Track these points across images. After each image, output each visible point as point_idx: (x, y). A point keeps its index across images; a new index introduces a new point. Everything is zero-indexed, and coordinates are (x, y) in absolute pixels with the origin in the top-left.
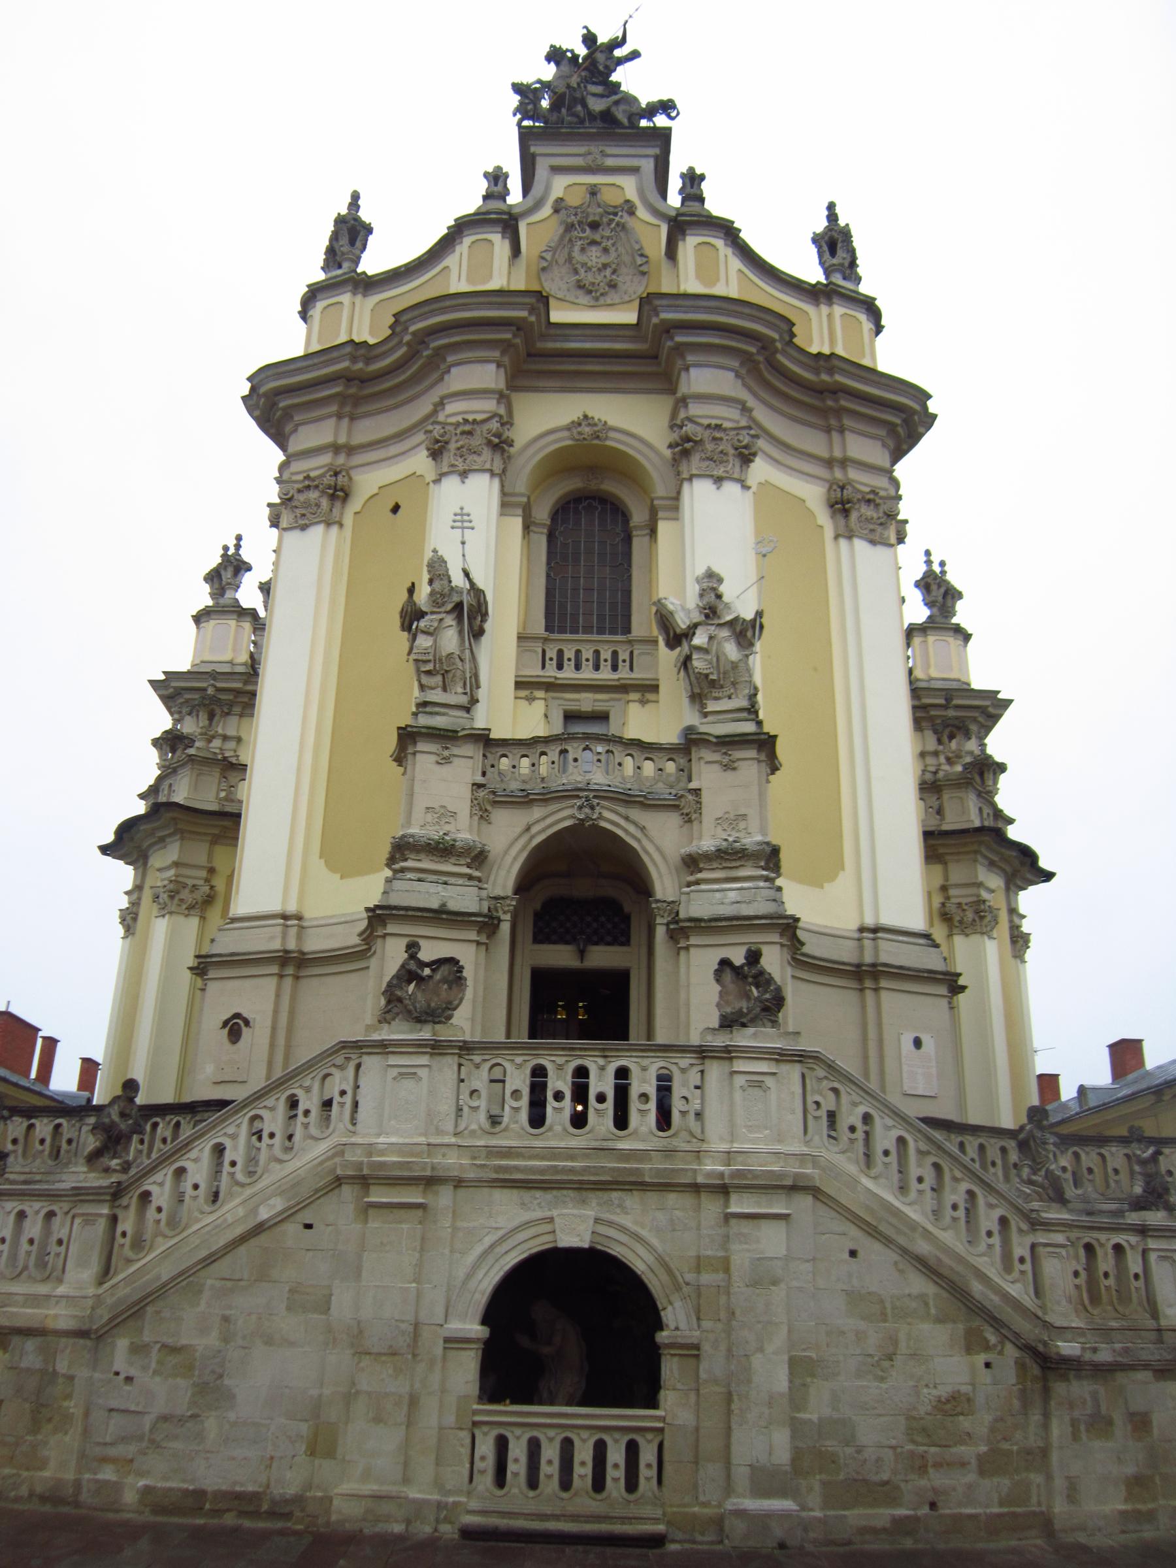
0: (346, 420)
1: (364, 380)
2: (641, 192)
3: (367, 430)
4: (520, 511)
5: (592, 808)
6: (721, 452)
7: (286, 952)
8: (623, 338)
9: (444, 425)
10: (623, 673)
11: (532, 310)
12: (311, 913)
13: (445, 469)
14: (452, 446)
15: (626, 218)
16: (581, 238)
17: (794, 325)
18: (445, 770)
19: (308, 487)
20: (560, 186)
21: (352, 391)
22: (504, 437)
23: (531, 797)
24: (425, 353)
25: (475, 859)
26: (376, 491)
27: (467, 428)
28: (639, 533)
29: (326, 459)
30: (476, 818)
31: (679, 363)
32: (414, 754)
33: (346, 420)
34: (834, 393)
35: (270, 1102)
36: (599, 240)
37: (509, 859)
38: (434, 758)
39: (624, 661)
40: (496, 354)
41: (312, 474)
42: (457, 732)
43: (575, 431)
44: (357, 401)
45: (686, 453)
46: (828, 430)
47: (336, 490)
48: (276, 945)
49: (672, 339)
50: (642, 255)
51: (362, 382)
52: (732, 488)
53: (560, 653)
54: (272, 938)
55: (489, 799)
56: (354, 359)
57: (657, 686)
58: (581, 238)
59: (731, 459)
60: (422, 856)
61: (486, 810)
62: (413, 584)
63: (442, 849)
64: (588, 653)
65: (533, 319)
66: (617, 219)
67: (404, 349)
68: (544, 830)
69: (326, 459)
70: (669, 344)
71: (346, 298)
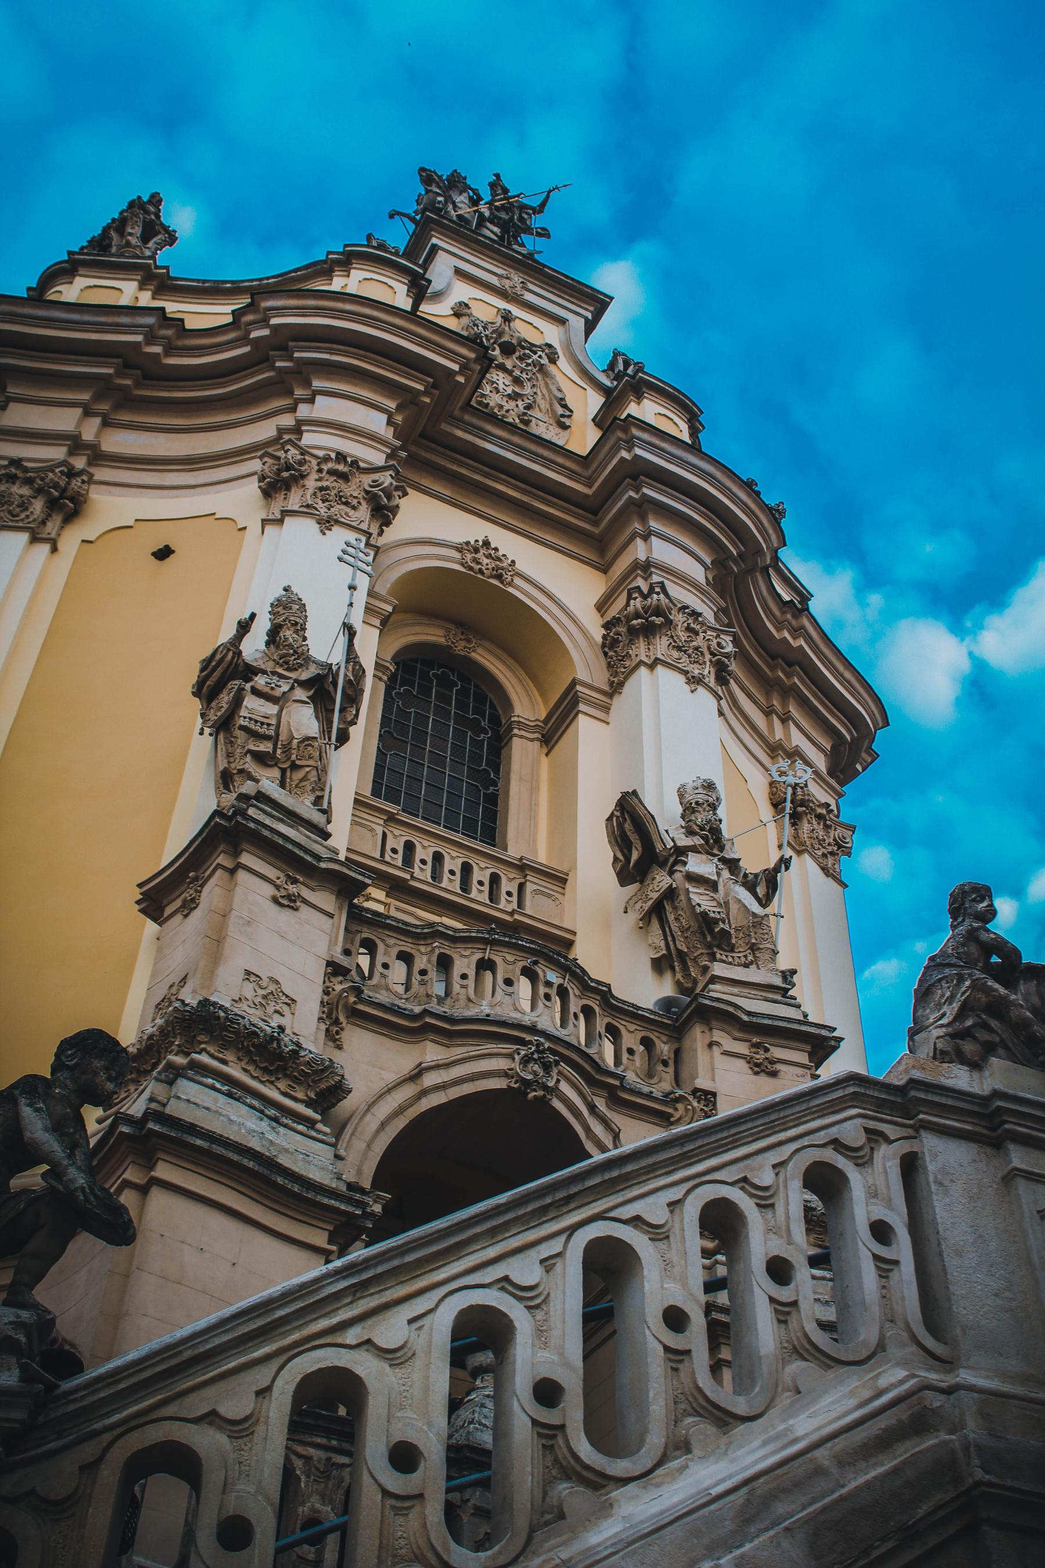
0: (97, 421)
1: (153, 373)
2: (568, 345)
4: (377, 622)
5: (547, 1067)
6: (697, 649)
8: (561, 469)
9: (303, 452)
11: (464, 368)
13: (296, 508)
14: (311, 483)
15: (545, 361)
17: (785, 545)
18: (284, 918)
20: (463, 292)
21: (128, 382)
22: (394, 503)
23: (428, 1020)
25: (321, 1094)
26: (131, 523)
27: (341, 467)
28: (523, 733)
29: (57, 453)
30: (323, 1027)
31: (637, 526)
32: (232, 872)
33: (97, 421)
34: (790, 665)
35: (653, 1209)
36: (509, 367)
37: (372, 1122)
38: (269, 890)
39: (509, 894)
40: (392, 405)
42: (319, 858)
43: (469, 557)
44: (127, 401)
45: (649, 631)
46: (768, 712)
47: (61, 497)
52: (705, 701)
53: (409, 847)
56: (151, 338)
59: (708, 663)
60: (230, 1056)
61: (337, 1022)
62: (253, 616)
64: (453, 862)
65: (461, 379)
66: (535, 357)
67: (247, 349)
68: (443, 1087)
69: (57, 453)
70: (632, 493)
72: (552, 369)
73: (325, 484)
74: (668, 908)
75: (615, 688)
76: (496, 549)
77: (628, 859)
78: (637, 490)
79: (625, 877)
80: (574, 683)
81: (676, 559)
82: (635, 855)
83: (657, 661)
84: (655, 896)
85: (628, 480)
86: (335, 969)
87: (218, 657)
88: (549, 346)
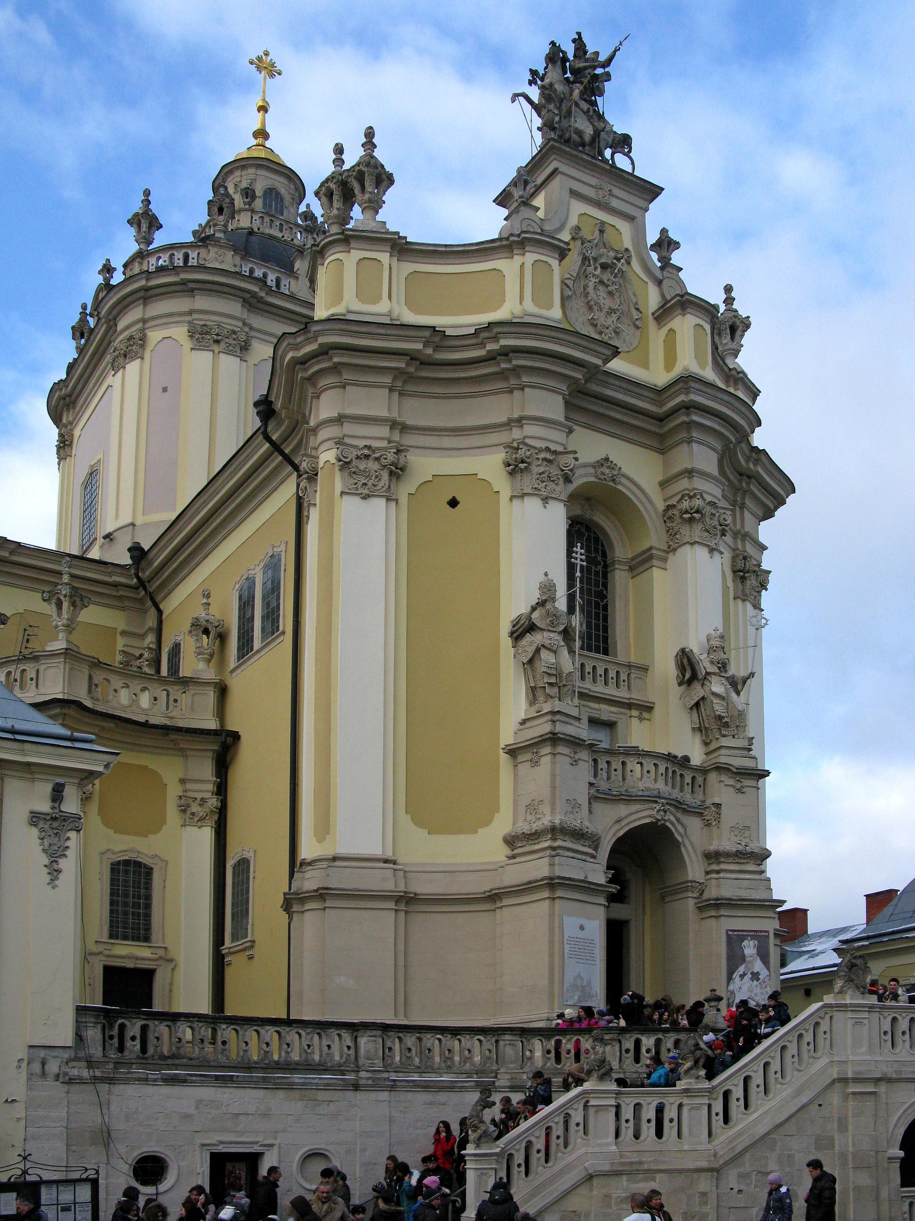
3: (417, 412)
7: (405, 892)
12: (406, 858)
38: (568, 760)
45: (691, 520)
48: (389, 886)
55: (598, 797)
63: (578, 835)
74: (701, 703)
76: (612, 462)
77: (684, 676)
80: (651, 548)
81: (703, 457)
82: (688, 676)
83: (696, 542)
84: (697, 699)
86: (591, 784)
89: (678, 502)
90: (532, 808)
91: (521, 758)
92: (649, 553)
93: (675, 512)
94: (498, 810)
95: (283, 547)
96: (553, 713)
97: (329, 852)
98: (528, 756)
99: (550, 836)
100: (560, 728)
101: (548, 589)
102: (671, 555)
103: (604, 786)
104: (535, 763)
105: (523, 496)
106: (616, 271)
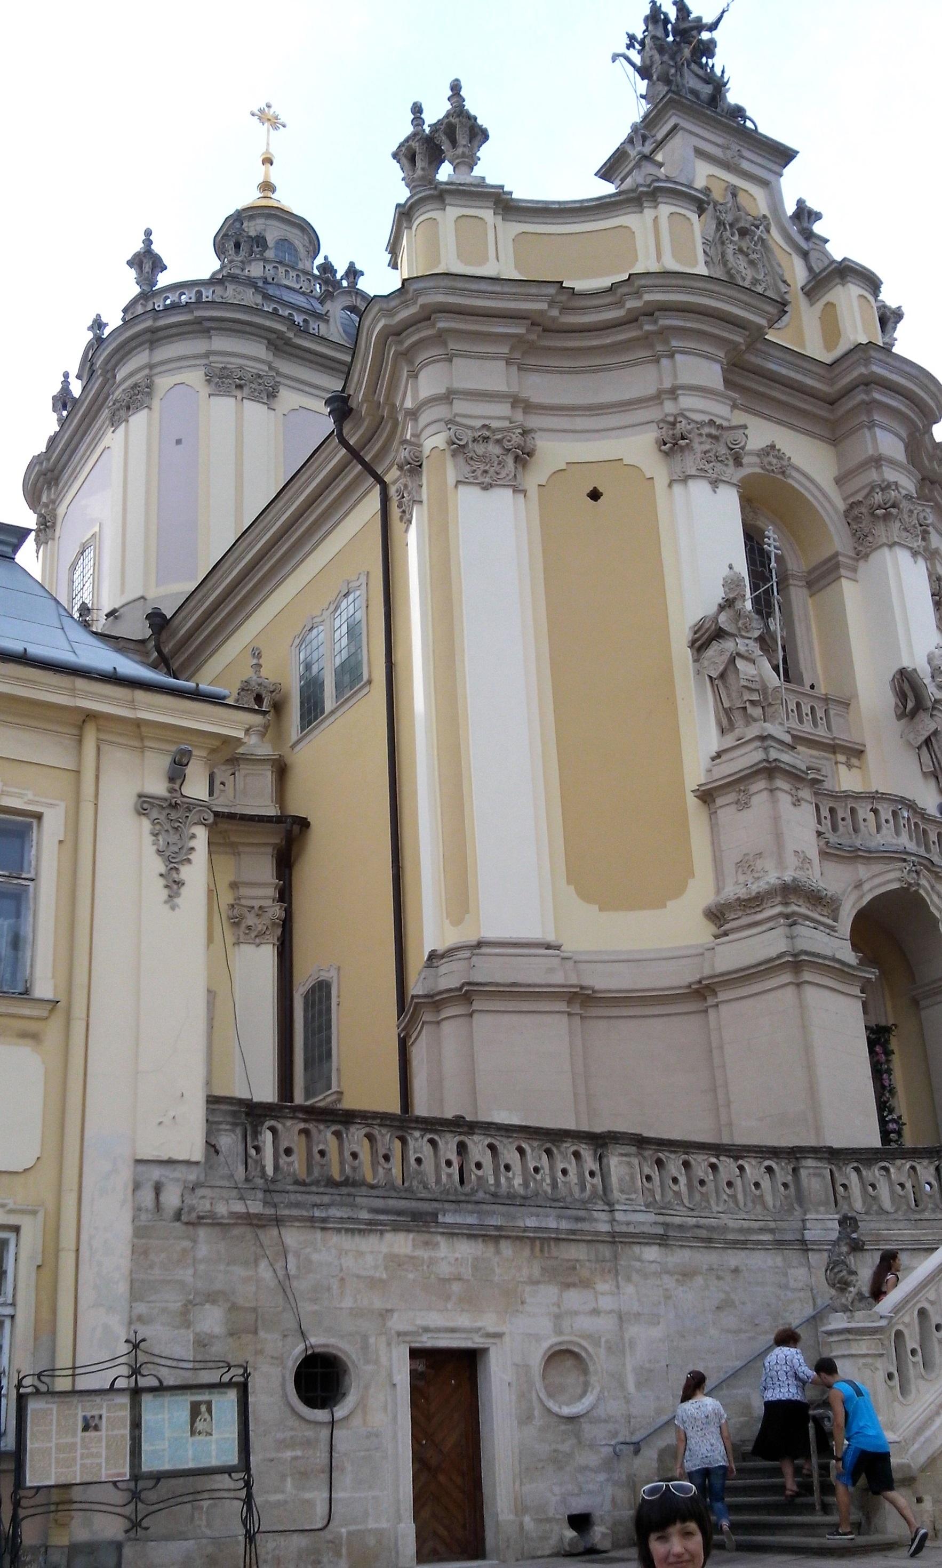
7: (582, 988)
9: (690, 421)
10: (821, 732)
13: (694, 472)
14: (698, 448)
16: (731, 242)
19: (486, 439)
23: (861, 853)
24: (647, 327)
27: (714, 431)
33: (514, 369)
41: (494, 424)
45: (887, 517)
49: (867, 393)
50: (785, 282)
51: (544, 330)
54: (551, 970)
56: (552, 304)
57: (862, 752)
58: (731, 242)
63: (816, 898)
66: (759, 232)
68: (871, 890)
69: (504, 409)
71: (487, 214)
72: (770, 242)
73: (707, 447)
75: (861, 555)
76: (779, 450)
78: (867, 393)
79: (900, 717)
80: (836, 555)
82: (910, 705)
84: (927, 734)
85: (862, 387)
86: (819, 834)
87: (707, 626)
88: (765, 216)
89: (866, 497)
90: (746, 865)
91: (720, 801)
92: (833, 562)
93: (864, 510)
94: (692, 875)
95: (363, 579)
96: (762, 738)
97: (473, 939)
98: (732, 797)
99: (779, 899)
100: (773, 754)
101: (732, 583)
102: (861, 564)
103: (833, 839)
104: (743, 805)
105: (686, 479)
106: (756, 238)
